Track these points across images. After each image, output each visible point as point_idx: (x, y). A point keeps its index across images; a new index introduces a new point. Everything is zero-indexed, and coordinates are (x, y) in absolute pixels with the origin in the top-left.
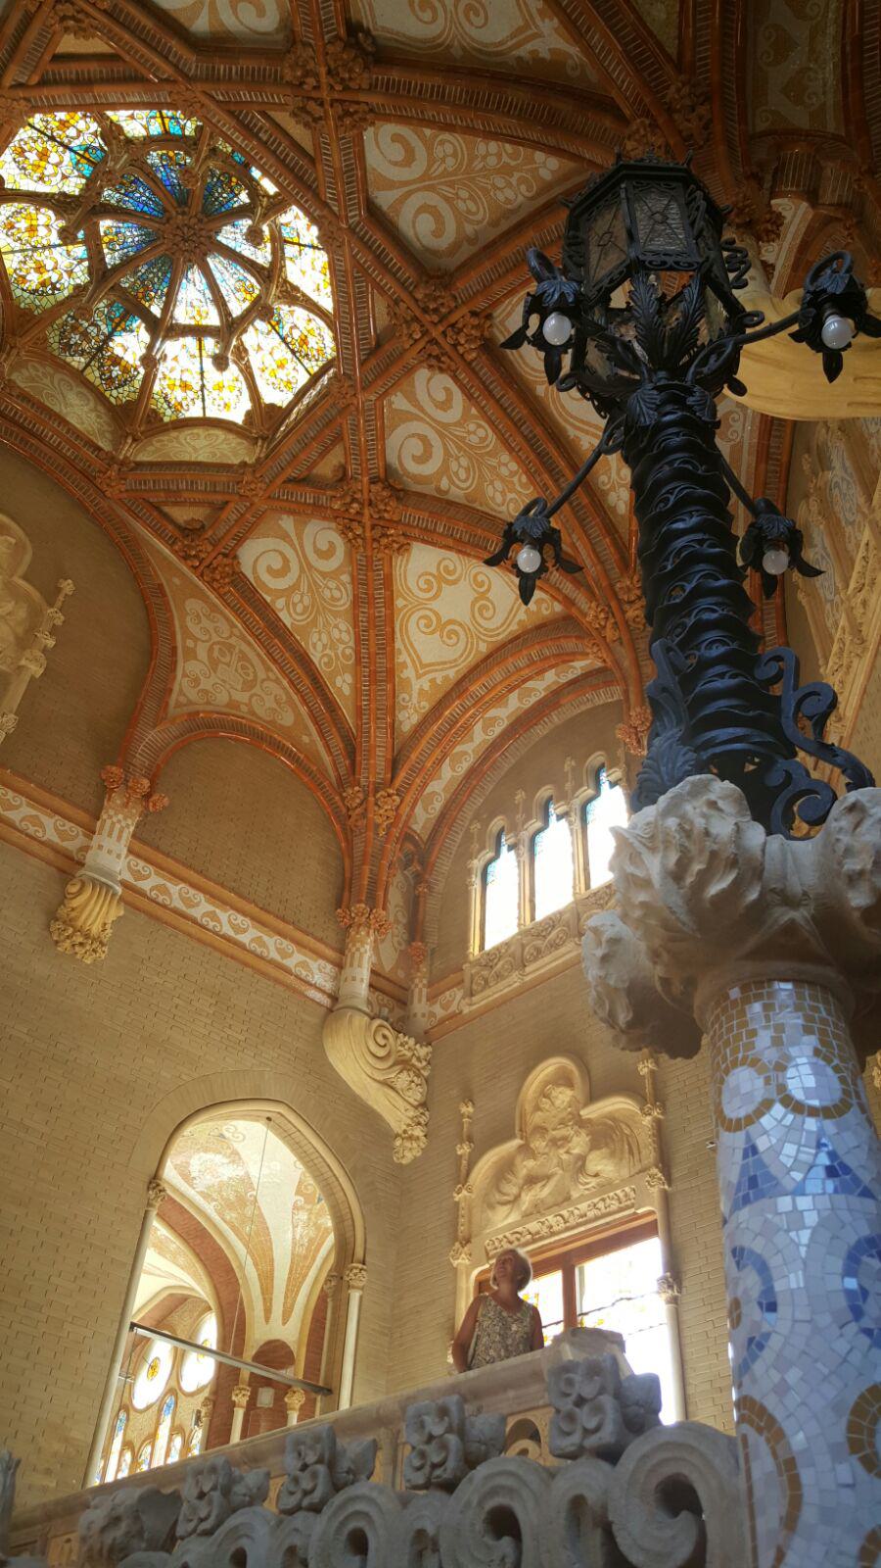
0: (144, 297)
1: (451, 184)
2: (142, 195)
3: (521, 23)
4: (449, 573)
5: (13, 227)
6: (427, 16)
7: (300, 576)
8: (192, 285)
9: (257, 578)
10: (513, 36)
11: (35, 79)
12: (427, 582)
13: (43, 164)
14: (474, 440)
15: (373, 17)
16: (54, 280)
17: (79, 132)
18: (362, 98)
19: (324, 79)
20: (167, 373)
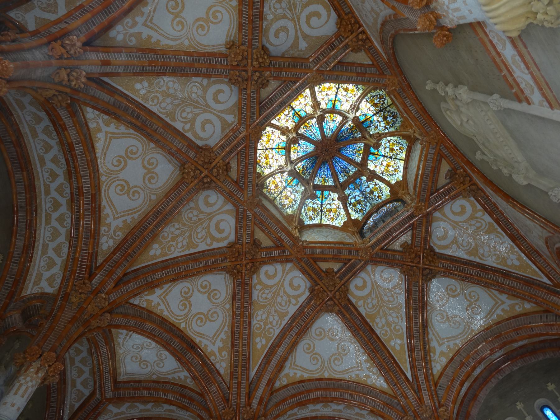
0: (353, 127)
1: (200, 219)
2: (340, 166)
3: (167, 297)
4: (202, 27)
5: (395, 169)
6: (205, 283)
7: (301, 13)
8: (331, 127)
9: (328, 11)
10: (170, 291)
11: (352, 261)
12: (215, 17)
13: (373, 190)
14: (188, 109)
15: (225, 278)
16: (388, 144)
17: (355, 198)
18: (229, 264)
19: (244, 267)
20: (353, 97)
